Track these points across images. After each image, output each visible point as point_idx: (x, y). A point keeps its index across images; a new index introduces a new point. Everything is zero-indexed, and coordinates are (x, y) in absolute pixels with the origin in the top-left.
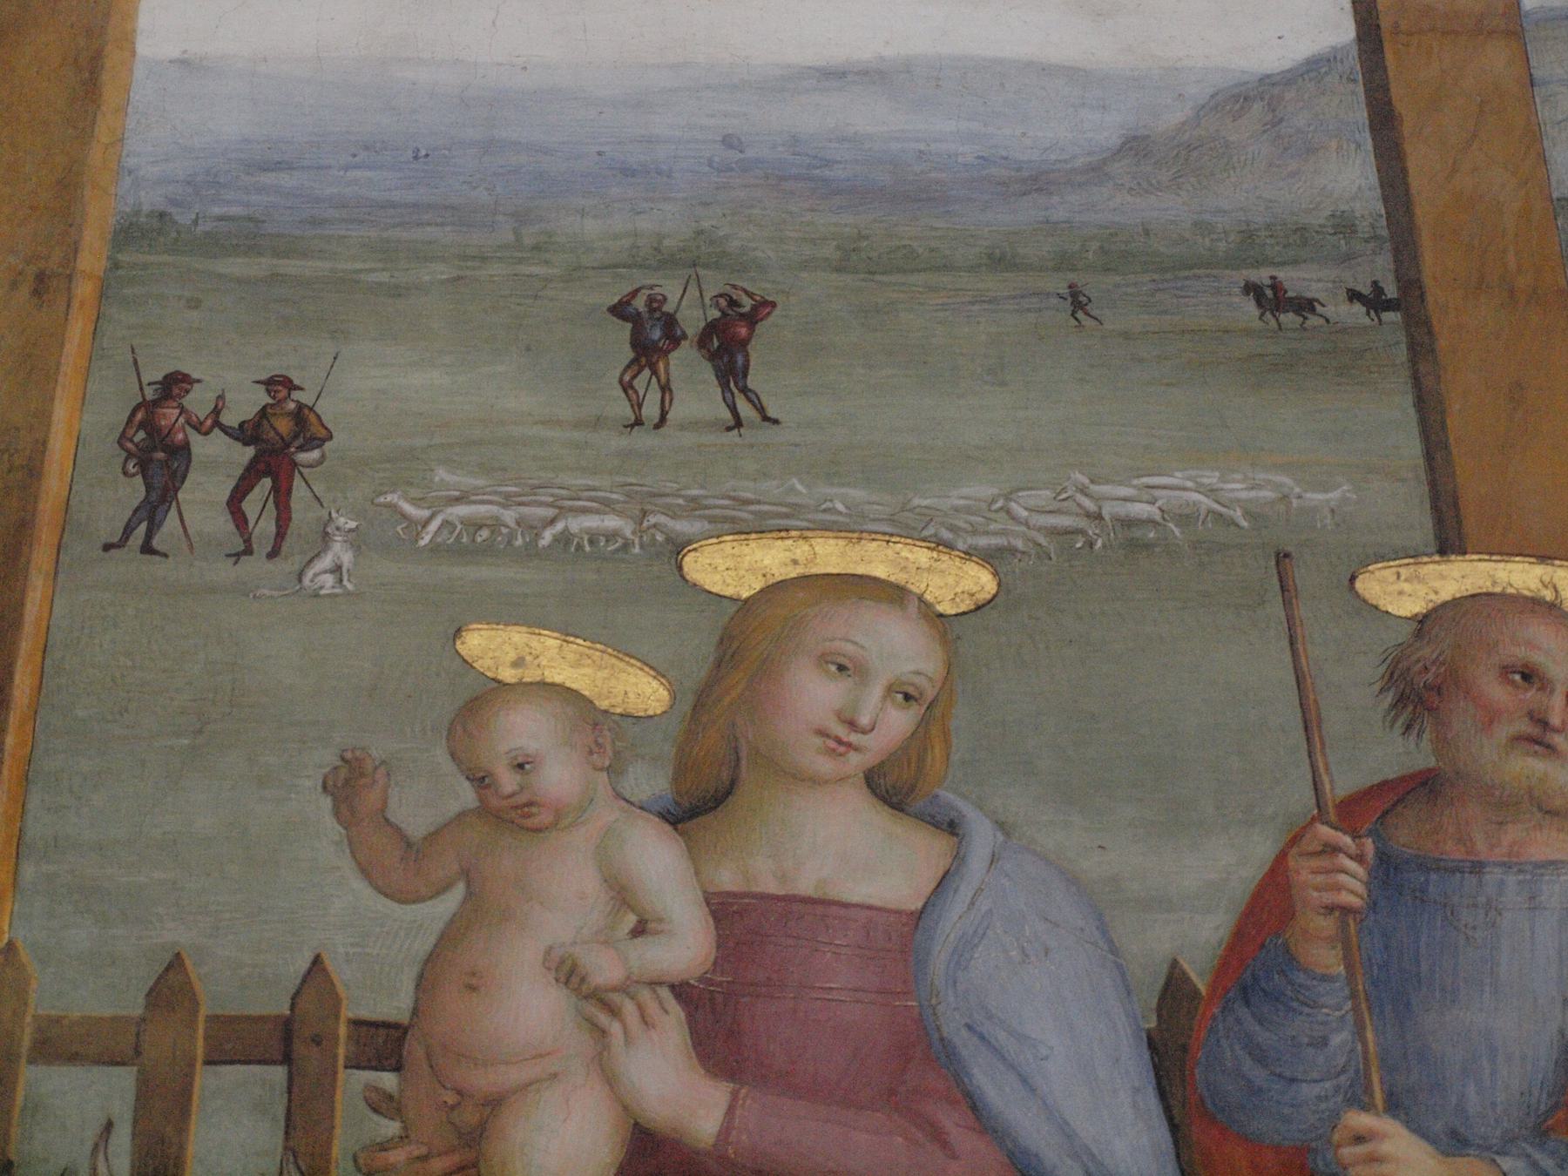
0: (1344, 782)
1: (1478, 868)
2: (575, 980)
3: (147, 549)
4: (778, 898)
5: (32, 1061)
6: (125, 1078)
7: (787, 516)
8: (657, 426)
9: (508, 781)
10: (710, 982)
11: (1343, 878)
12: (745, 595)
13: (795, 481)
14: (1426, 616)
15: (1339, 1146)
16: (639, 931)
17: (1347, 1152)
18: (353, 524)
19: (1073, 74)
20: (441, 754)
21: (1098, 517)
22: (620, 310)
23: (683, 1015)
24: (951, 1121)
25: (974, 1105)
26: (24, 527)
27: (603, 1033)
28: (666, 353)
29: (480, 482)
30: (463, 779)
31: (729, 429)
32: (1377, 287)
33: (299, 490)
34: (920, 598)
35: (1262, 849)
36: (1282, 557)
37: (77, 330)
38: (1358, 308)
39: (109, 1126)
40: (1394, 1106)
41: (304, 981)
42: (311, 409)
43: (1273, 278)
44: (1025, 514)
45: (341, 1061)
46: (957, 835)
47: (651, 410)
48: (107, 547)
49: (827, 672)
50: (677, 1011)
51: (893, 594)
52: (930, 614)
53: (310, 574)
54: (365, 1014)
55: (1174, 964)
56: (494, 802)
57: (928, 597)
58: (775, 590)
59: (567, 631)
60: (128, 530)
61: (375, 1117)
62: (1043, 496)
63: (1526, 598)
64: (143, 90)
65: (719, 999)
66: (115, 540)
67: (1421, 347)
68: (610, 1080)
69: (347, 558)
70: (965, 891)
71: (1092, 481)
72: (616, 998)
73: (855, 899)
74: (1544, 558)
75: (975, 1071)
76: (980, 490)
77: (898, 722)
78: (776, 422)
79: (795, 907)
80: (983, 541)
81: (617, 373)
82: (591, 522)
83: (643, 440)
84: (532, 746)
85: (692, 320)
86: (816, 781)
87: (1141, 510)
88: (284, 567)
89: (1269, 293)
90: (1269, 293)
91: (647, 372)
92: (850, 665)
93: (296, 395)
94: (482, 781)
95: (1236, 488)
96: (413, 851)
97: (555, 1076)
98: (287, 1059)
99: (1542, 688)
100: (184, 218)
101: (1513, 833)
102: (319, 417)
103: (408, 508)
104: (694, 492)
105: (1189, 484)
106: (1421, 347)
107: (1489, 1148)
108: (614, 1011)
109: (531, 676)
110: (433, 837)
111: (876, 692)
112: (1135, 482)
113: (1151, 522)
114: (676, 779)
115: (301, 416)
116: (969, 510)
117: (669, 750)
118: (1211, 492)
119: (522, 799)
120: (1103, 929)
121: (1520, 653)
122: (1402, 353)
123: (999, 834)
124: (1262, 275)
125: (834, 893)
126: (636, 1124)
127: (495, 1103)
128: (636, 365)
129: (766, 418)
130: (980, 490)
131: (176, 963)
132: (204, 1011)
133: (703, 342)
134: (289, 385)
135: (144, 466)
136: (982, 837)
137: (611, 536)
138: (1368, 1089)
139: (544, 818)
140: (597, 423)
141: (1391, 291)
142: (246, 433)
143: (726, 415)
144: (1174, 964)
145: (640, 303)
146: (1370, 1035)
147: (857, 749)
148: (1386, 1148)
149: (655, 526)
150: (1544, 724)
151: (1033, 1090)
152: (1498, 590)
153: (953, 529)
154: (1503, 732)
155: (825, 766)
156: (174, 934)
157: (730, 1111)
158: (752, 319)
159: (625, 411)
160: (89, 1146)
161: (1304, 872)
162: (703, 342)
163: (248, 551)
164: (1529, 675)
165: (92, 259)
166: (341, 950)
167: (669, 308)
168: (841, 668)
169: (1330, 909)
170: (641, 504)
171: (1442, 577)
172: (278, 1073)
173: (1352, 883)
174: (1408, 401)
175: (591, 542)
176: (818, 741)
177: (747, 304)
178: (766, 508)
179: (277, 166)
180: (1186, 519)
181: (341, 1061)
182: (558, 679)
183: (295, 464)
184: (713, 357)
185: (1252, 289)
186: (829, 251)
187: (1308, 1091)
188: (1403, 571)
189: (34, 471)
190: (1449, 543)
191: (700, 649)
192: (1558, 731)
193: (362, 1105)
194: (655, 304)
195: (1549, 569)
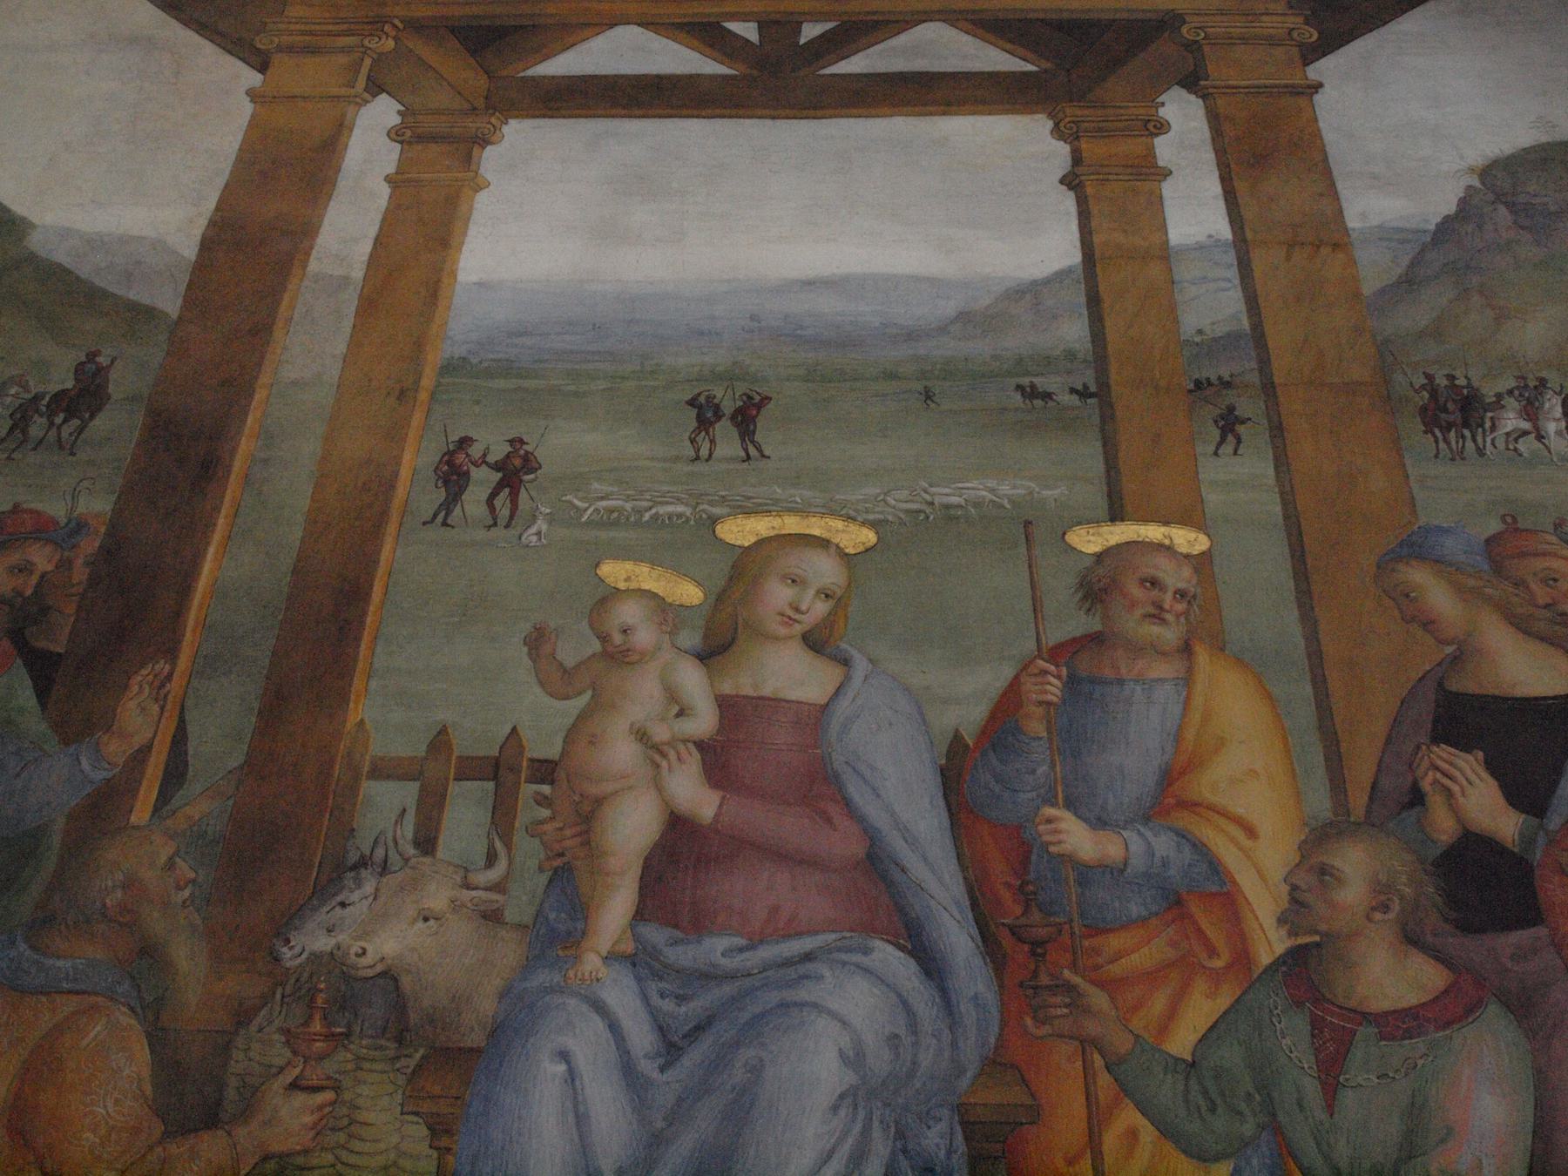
1: (1121, 682)
2: (645, 738)
3: (445, 524)
4: (753, 698)
5: (368, 778)
6: (413, 788)
7: (773, 505)
8: (707, 460)
9: (618, 638)
10: (715, 740)
11: (1049, 687)
12: (746, 545)
13: (776, 487)
14: (1101, 553)
15: (1039, 824)
16: (681, 713)
17: (1042, 828)
18: (548, 511)
19: (931, 281)
20: (585, 623)
21: (932, 504)
22: (692, 403)
23: (699, 757)
24: (834, 810)
25: (847, 804)
26: (384, 515)
27: (658, 766)
28: (712, 424)
29: (616, 489)
30: (595, 638)
31: (744, 461)
32: (1085, 386)
33: (523, 495)
34: (837, 546)
35: (1008, 672)
36: (1028, 523)
37: (417, 419)
38: (1075, 397)
39: (404, 810)
40: (1070, 804)
41: (507, 738)
42: (532, 454)
43: (1031, 382)
44: (893, 502)
45: (523, 779)
46: (846, 665)
47: (704, 452)
48: (424, 523)
49: (787, 585)
50: (697, 755)
51: (823, 543)
52: (843, 555)
53: (525, 535)
54: (536, 755)
55: (957, 731)
56: (610, 649)
57: (841, 545)
58: (762, 542)
59: (654, 563)
60: (435, 516)
61: (540, 808)
62: (904, 494)
63: (1155, 543)
64: (460, 297)
65: (719, 750)
66: (429, 519)
67: (1108, 416)
68: (659, 789)
69: (544, 528)
70: (851, 694)
71: (931, 486)
72: (665, 748)
73: (794, 698)
74: (1166, 523)
75: (849, 785)
76: (872, 490)
77: (821, 608)
78: (769, 457)
79: (761, 702)
80: (871, 517)
81: (688, 434)
82: (670, 509)
83: (699, 467)
84: (630, 621)
85: (728, 407)
86: (777, 639)
87: (955, 500)
88: (513, 532)
89: (1028, 389)
90: (1028, 389)
91: (703, 433)
92: (796, 578)
93: (525, 447)
94: (604, 638)
95: (1005, 489)
97: (630, 788)
98: (495, 778)
99: (1161, 590)
100: (474, 361)
101: (1140, 664)
102: (535, 458)
103: (577, 502)
104: (723, 493)
105: (981, 487)
107: (1117, 826)
108: (664, 755)
109: (633, 585)
110: (578, 666)
111: (811, 592)
112: (953, 486)
113: (959, 506)
114: (706, 637)
115: (527, 458)
116: (865, 501)
117: (702, 623)
118: (992, 491)
119: (627, 646)
120: (921, 714)
121: (1152, 572)
122: (1096, 419)
123: (871, 665)
124: (1025, 381)
125: (781, 695)
126: (672, 812)
127: (599, 801)
128: (698, 430)
129: (763, 456)
130: (872, 490)
131: (443, 731)
132: (456, 753)
133: (733, 418)
134: (522, 442)
135: (446, 483)
136: (861, 666)
137: (679, 516)
138: (1056, 796)
139: (636, 657)
140: (677, 459)
141: (1093, 389)
142: (497, 467)
143: (743, 454)
144: (957, 731)
145: (702, 399)
146: (1058, 769)
147: (798, 622)
148: (1063, 826)
149: (703, 510)
150: (1161, 608)
151: (878, 796)
152: (1140, 539)
153: (856, 511)
154: (1139, 612)
155: (783, 631)
157: (721, 805)
158: (759, 407)
159: (692, 453)
160: (393, 820)
161: (1029, 685)
162: (733, 418)
163: (495, 524)
164: (1154, 583)
165: (427, 382)
166: (527, 723)
167: (716, 401)
168: (793, 581)
169: (1041, 703)
171: (1112, 533)
172: (491, 785)
173: (1054, 689)
174: (1099, 444)
175: (669, 518)
176: (779, 618)
177: (757, 398)
178: (760, 501)
179: (524, 334)
180: (977, 505)
181: (523, 779)
182: (647, 588)
183: (521, 481)
184: (737, 425)
185: (1019, 388)
186: (802, 372)
187: (1022, 797)
188: (1091, 531)
189: (391, 486)
192: (1168, 612)
193: (533, 803)
194: (710, 399)
195: (1168, 529)
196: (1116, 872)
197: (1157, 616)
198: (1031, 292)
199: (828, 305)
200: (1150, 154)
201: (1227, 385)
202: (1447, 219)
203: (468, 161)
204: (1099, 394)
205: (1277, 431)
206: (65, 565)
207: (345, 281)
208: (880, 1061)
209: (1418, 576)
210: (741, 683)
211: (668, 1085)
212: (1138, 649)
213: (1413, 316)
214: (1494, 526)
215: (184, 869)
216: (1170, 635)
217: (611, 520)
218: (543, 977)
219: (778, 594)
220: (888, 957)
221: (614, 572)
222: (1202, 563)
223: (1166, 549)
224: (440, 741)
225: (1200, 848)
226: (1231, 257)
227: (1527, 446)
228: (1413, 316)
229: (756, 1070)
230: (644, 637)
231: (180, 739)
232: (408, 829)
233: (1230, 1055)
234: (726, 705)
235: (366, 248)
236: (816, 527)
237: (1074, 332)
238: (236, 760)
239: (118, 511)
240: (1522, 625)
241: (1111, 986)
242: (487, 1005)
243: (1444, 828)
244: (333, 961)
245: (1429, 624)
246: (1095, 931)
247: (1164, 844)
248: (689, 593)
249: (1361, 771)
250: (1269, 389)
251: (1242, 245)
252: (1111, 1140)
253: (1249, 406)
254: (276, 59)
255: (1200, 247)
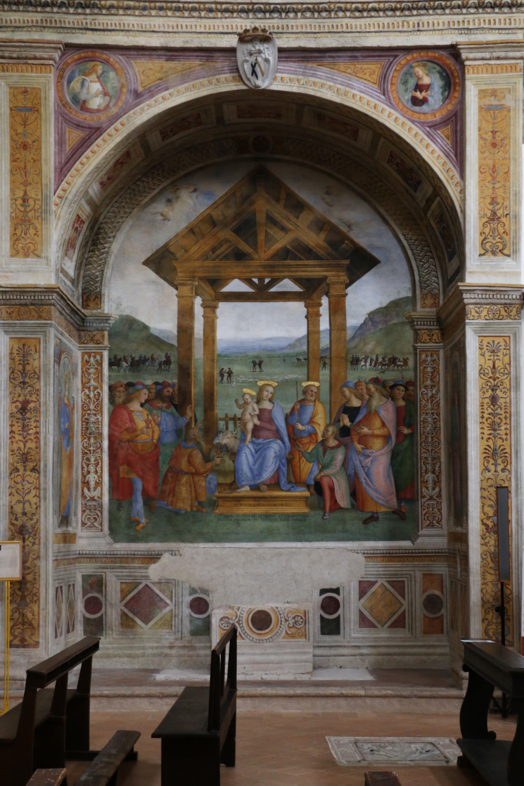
0: (299, 399)
51: (270, 385)
67: (308, 364)
76: (277, 377)
77: (270, 395)
85: (258, 362)
96: (240, 406)
106: (308, 364)
127: (246, 423)
130: (277, 377)
142: (228, 373)
156: (226, 412)
164: (312, 391)
165: (216, 357)
170: (254, 378)
173: (298, 407)
189: (214, 377)
190: (308, 380)
191: (258, 390)
196: (304, 431)
197: (312, 396)
198: (299, 340)
199: (271, 344)
200: (319, 311)
201: (325, 357)
202: (362, 324)
203: (214, 312)
204: (307, 359)
205: (331, 365)
206: (174, 391)
207: (200, 339)
208: (278, 453)
209: (345, 389)
210: (262, 407)
211: (256, 456)
212: (310, 401)
213: (353, 344)
214: (357, 381)
215: (200, 433)
216: (313, 399)
217: (243, 382)
218: (242, 445)
219: (265, 393)
220: (279, 441)
221: (245, 390)
222: (318, 388)
223: (314, 385)
224: (226, 415)
225: (314, 428)
226: (328, 333)
227: (364, 367)
228: (353, 344)
229: (265, 454)
230: (249, 400)
231: (195, 416)
232: (225, 427)
233: (314, 452)
234: (261, 410)
235: (202, 332)
236: (269, 383)
237: (305, 348)
238: (202, 418)
239: (178, 382)
240: (356, 397)
241: (302, 444)
242: (236, 448)
243: (342, 424)
244: (219, 443)
245: (345, 397)
246: (301, 438)
247: (310, 427)
248: (254, 393)
249: (334, 417)
250: (331, 358)
251: (330, 330)
252: (301, 461)
253: (327, 361)
254: (179, 287)
255: (324, 331)
